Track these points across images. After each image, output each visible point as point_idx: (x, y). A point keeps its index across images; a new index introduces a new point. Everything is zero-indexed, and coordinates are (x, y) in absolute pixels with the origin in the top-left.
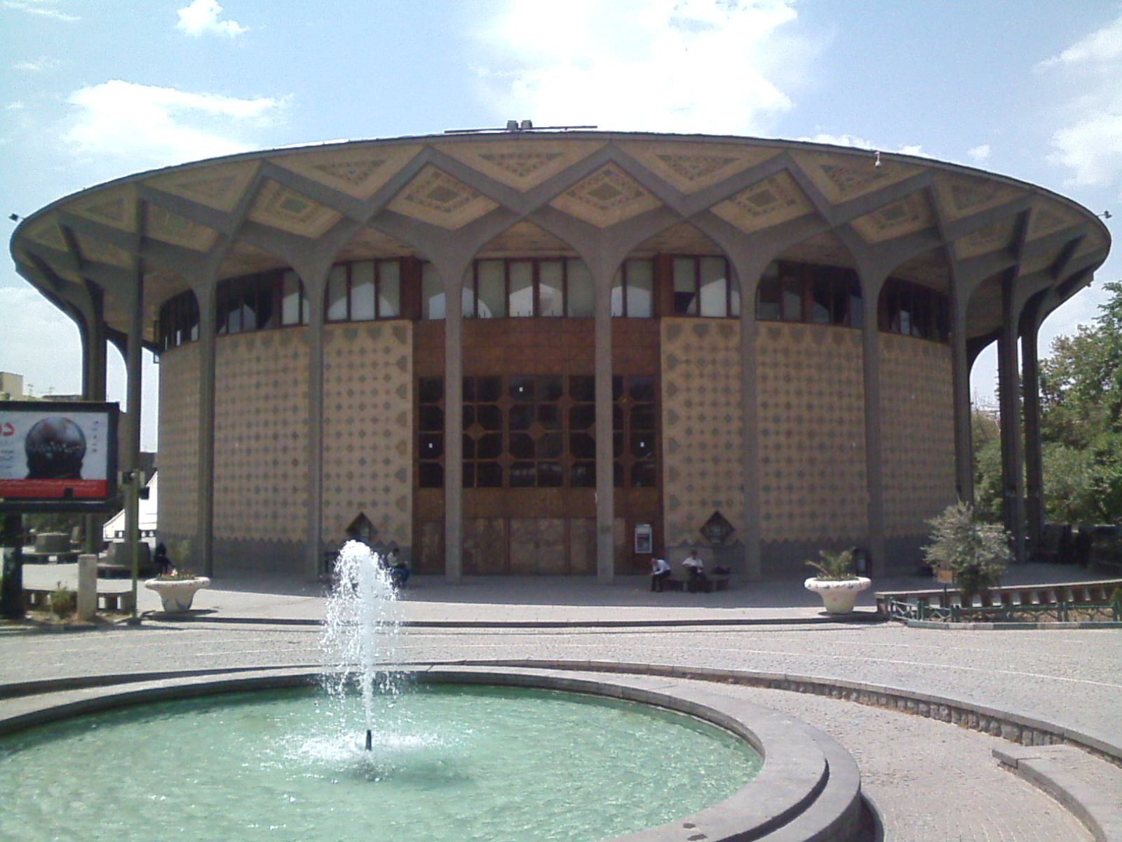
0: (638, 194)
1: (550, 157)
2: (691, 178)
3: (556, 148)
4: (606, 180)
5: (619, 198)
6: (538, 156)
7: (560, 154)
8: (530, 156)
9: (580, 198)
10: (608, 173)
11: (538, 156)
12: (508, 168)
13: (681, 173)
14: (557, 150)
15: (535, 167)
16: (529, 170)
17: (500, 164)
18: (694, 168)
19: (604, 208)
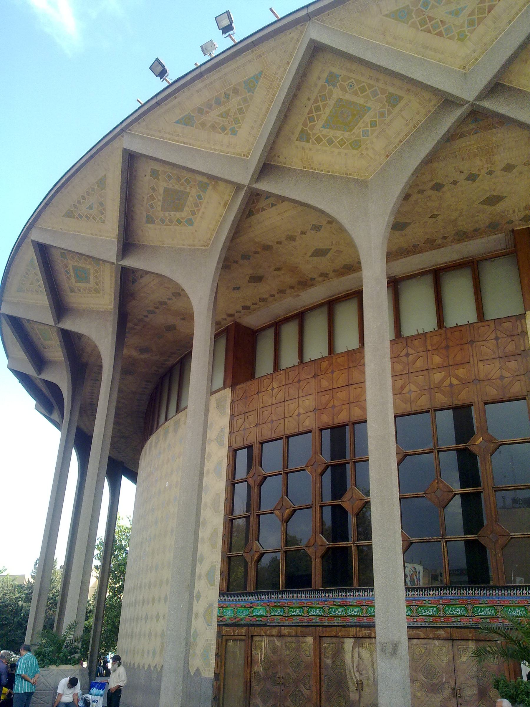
0: (393, 101)
1: (251, 85)
2: (462, 38)
3: (249, 66)
4: (337, 93)
5: (367, 118)
6: (236, 91)
7: (257, 78)
8: (227, 96)
9: (319, 140)
10: (332, 79)
11: (236, 91)
12: (213, 127)
13: (440, 34)
14: (252, 70)
15: (241, 111)
16: (237, 121)
17: (203, 125)
18: (456, 13)
19: (356, 145)
